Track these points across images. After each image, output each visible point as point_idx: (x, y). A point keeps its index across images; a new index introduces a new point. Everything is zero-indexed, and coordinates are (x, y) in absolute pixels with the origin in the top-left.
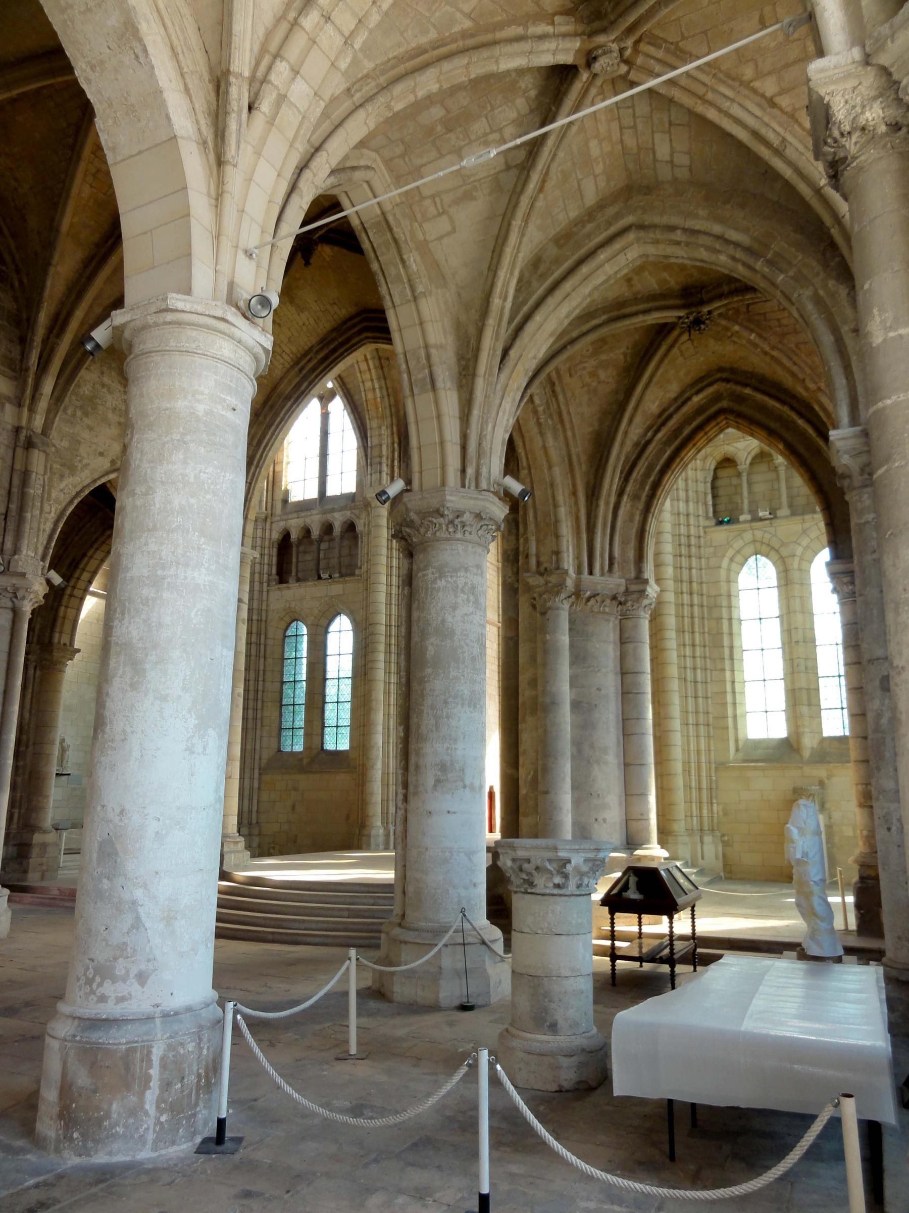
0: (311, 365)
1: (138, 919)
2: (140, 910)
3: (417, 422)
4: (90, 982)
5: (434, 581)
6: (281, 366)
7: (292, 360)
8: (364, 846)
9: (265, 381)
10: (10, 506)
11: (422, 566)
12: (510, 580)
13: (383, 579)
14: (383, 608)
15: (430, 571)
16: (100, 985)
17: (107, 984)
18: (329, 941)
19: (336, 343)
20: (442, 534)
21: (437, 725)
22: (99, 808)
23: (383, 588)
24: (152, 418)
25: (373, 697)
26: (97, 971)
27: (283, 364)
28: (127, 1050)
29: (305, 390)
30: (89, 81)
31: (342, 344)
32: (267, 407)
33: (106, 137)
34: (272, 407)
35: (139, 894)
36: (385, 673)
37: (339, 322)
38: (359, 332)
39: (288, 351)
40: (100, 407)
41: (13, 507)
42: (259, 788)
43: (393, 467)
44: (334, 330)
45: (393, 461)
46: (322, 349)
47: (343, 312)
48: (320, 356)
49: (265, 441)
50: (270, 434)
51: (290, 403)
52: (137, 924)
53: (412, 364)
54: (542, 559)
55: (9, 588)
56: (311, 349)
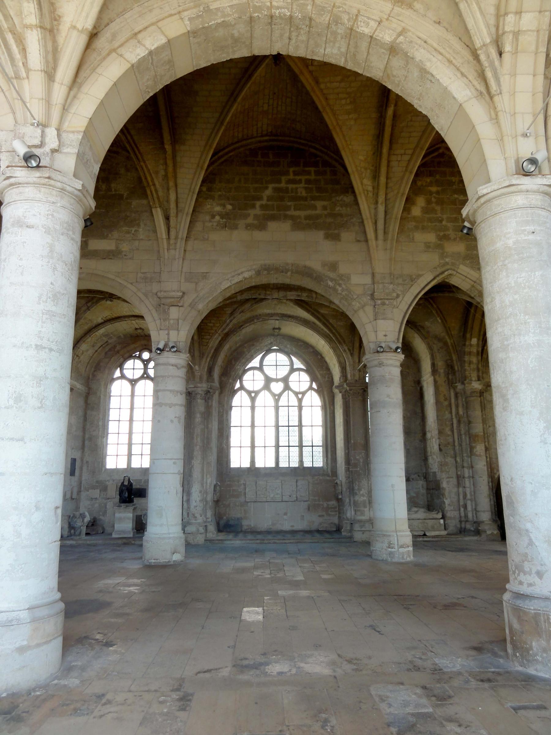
1: (530, 540)
2: (531, 535)
16: (519, 575)
17: (522, 575)
24: (487, 259)
26: (516, 567)
28: (535, 613)
30: (420, 106)
35: (529, 526)
52: (531, 543)
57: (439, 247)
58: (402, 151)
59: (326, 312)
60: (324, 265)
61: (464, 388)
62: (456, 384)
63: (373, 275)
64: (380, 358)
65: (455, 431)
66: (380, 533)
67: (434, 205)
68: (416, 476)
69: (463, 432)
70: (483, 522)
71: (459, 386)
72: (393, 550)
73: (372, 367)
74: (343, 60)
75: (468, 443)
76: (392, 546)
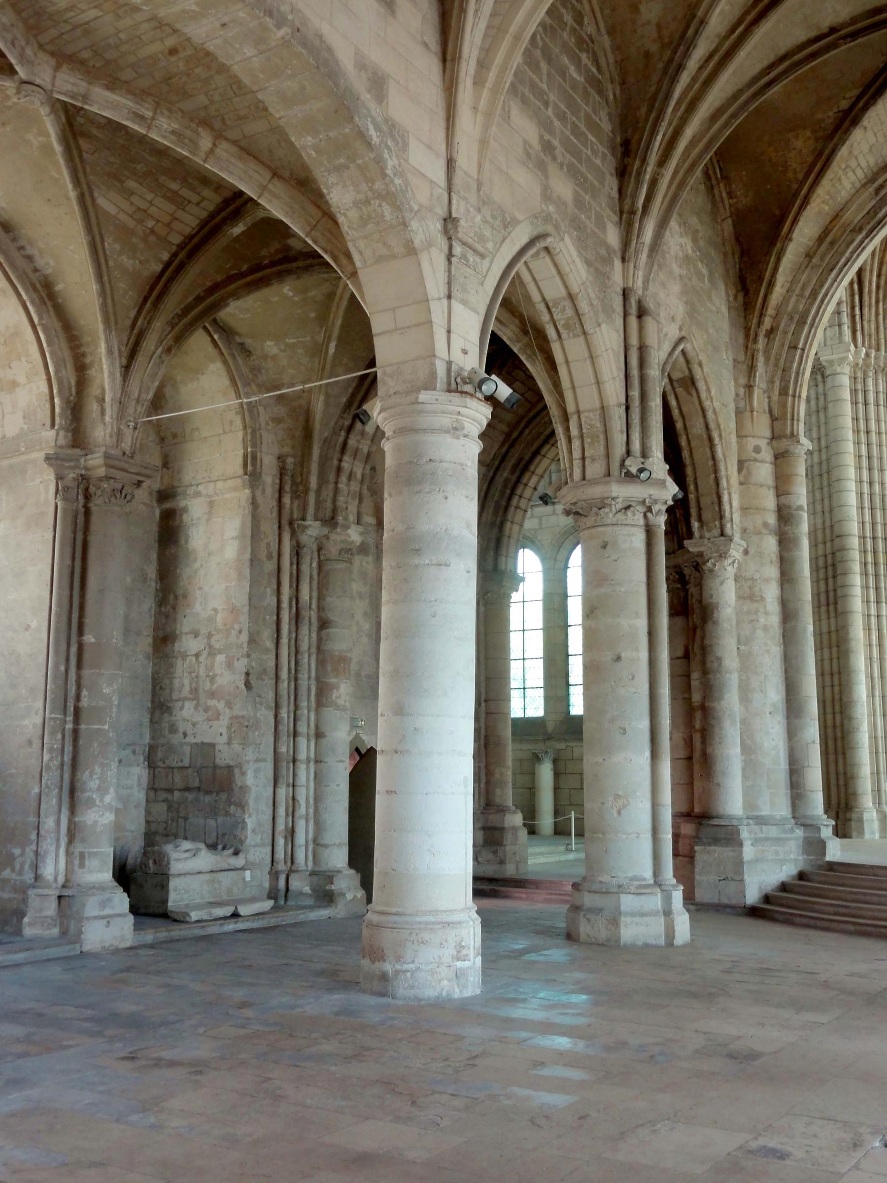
6: (850, 186)
7: (866, 176)
8: (854, 834)
9: (826, 208)
10: (631, 393)
13: (851, 473)
14: (853, 512)
23: (852, 486)
25: (852, 635)
27: (853, 184)
32: (824, 246)
34: (832, 243)
36: (863, 602)
39: (863, 164)
40: (667, 256)
41: (635, 393)
43: (853, 317)
45: (853, 308)
49: (824, 290)
50: (830, 281)
51: (861, 237)
55: (647, 501)
57: (541, 166)
59: (112, 210)
60: (361, 65)
61: (327, 537)
62: (306, 523)
63: (450, 164)
64: (464, 411)
65: (284, 640)
66: (431, 919)
67: (538, 53)
68: (128, 751)
69: (304, 646)
70: (339, 872)
71: (313, 529)
72: (467, 964)
73: (433, 431)
75: (313, 674)
76: (464, 952)
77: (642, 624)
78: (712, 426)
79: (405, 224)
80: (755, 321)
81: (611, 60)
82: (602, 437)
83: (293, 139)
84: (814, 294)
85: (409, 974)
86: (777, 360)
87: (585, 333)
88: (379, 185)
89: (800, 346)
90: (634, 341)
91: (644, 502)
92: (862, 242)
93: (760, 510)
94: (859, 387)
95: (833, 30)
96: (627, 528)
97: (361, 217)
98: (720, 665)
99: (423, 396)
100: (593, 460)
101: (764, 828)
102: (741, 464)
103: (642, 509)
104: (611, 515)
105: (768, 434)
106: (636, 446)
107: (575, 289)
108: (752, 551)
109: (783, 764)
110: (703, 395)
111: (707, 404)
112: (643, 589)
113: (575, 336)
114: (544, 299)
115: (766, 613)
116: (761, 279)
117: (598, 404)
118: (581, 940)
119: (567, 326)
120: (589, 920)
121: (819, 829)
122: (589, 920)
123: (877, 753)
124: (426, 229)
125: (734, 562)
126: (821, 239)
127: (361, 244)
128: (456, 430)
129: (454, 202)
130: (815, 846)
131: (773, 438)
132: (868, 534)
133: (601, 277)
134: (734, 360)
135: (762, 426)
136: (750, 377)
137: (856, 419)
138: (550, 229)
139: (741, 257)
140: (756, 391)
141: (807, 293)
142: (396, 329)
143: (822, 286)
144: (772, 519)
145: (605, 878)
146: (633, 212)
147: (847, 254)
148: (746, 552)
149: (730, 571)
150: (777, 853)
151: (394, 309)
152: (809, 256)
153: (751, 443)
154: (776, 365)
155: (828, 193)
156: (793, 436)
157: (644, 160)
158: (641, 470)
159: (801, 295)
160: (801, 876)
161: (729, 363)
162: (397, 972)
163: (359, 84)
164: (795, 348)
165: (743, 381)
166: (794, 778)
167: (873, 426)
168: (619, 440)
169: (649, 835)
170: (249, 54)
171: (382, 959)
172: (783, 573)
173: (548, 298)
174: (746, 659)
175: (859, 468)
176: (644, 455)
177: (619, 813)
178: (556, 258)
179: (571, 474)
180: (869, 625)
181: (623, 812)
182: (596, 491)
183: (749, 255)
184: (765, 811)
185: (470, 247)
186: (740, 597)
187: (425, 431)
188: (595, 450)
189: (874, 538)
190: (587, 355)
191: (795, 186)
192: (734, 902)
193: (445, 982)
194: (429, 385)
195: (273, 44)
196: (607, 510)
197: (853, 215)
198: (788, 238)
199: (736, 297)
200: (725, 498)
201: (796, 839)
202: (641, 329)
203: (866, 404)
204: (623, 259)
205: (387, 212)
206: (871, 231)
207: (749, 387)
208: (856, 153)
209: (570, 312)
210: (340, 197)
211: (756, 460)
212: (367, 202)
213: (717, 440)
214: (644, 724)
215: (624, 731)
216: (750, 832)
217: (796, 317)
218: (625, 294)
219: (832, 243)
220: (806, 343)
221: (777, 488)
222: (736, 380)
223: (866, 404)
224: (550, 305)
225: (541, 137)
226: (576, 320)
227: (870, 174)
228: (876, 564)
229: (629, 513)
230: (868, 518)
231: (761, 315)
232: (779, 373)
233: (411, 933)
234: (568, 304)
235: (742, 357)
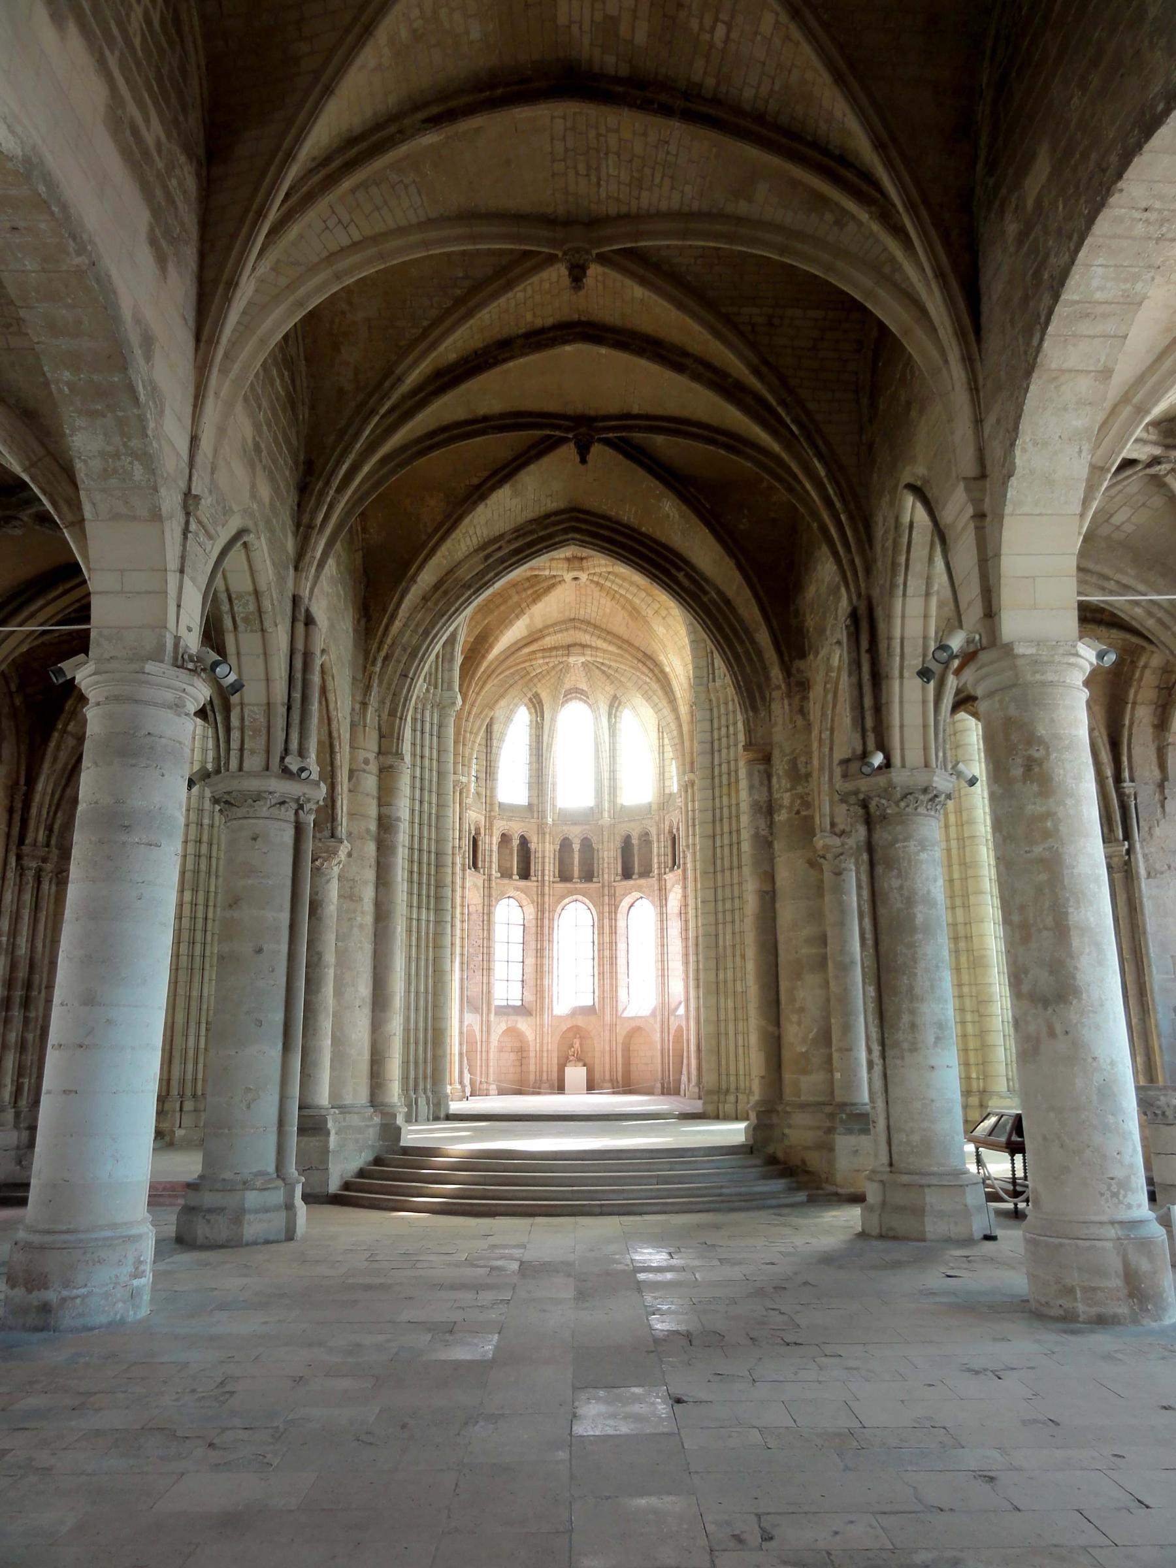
0: (500, 554)
3: (901, 702)
4: (1115, 1195)
5: (917, 853)
11: (901, 837)
12: (763, 833)
15: (912, 843)
16: (1125, 1196)
18: (669, 1208)
19: (536, 536)
20: (921, 810)
21: (932, 986)
22: (1090, 1060)
24: (1067, 742)
29: (489, 581)
30: (1024, 450)
31: (542, 539)
33: (1015, 493)
34: (445, 593)
37: (542, 514)
38: (565, 531)
39: (479, 534)
41: (297, 695)
42: (206, 1049)
44: (531, 521)
46: (516, 538)
47: (552, 505)
48: (512, 547)
50: (440, 624)
53: (907, 650)
54: (837, 820)
56: (502, 536)
58: (346, 218)
64: (189, 688)
66: (109, 1234)
74: (1076, 297)
76: (142, 1268)
77: (285, 917)
78: (335, 734)
79: (156, 489)
80: (375, 646)
81: (305, 385)
82: (264, 731)
83: (46, 369)
84: (426, 633)
85: (78, 1301)
86: (389, 685)
87: (263, 630)
88: (135, 443)
89: (410, 675)
90: (300, 646)
91: (297, 800)
92: (470, 597)
93: (365, 816)
94: (419, 716)
95: (485, 418)
96: (280, 823)
97: (105, 470)
98: (320, 959)
99: (150, 667)
100: (252, 752)
101: (348, 1116)
102: (352, 773)
103: (295, 806)
104: (265, 809)
105: (376, 749)
106: (294, 745)
107: (263, 586)
108: (355, 854)
109: (366, 1056)
110: (332, 706)
111: (333, 713)
112: (289, 883)
113: (252, 631)
114: (227, 590)
115: (363, 913)
116: (385, 610)
117: (265, 701)
118: (198, 1243)
119: (246, 620)
120: (208, 1221)
121: (395, 1116)
122: (208, 1221)
123: (408, 1043)
124: (170, 500)
125: (339, 863)
126: (437, 586)
127: (98, 497)
128: (177, 707)
129: (194, 478)
130: (391, 1132)
131: (379, 753)
132: (416, 846)
133: (281, 579)
134: (354, 678)
135: (371, 742)
136: (365, 695)
137: (414, 744)
138: (250, 524)
139: (367, 587)
140: (370, 710)
141: (421, 631)
142: (122, 592)
143: (433, 627)
144: (373, 827)
145: (227, 1175)
146: (310, 527)
147: (457, 605)
148: (349, 855)
149: (336, 870)
150: (357, 1141)
151: (122, 571)
152: (425, 599)
153: (362, 755)
154: (388, 689)
155: (448, 549)
156: (399, 755)
157: (327, 483)
158: (302, 770)
159: (415, 631)
160: (378, 1161)
161: (349, 679)
162: (64, 1300)
163: (134, 338)
164: (406, 676)
165: (359, 698)
166: (375, 1068)
167: (427, 753)
168: (280, 735)
169: (275, 1129)
170: (29, 267)
171: (45, 1286)
172: (378, 877)
173: (232, 590)
174: (341, 953)
175: (413, 787)
176: (302, 753)
177: (248, 1107)
178: (252, 554)
179: (227, 763)
180: (410, 927)
181: (252, 1106)
182: (253, 784)
183: (376, 589)
184: (348, 1100)
185: (203, 527)
186: (340, 896)
187: (147, 703)
188: (255, 744)
189: (420, 850)
190: (261, 651)
191: (424, 537)
192: (317, 1190)
193: (120, 1305)
194: (156, 655)
195: (65, 268)
196: (261, 803)
197: (465, 574)
198: (413, 579)
199: (359, 621)
200: (339, 803)
201: (374, 1126)
202: (307, 636)
203: (422, 733)
204: (296, 568)
205: (138, 471)
206: (478, 589)
207: (364, 705)
208: (475, 522)
209: (252, 607)
210: (85, 443)
211: (364, 771)
212: (117, 456)
213: (337, 749)
214: (279, 1017)
215: (260, 1023)
216: (335, 1121)
217: (409, 651)
218: (296, 600)
219: (445, 593)
220: (415, 674)
221: (379, 799)
222: (353, 696)
223: (422, 733)
224: (234, 596)
225: (254, 438)
226: (257, 614)
227: (481, 542)
228: (420, 873)
229: (283, 809)
230: (416, 833)
231: (381, 643)
232: (390, 697)
233: (85, 1253)
234: (252, 599)
235: (360, 676)
